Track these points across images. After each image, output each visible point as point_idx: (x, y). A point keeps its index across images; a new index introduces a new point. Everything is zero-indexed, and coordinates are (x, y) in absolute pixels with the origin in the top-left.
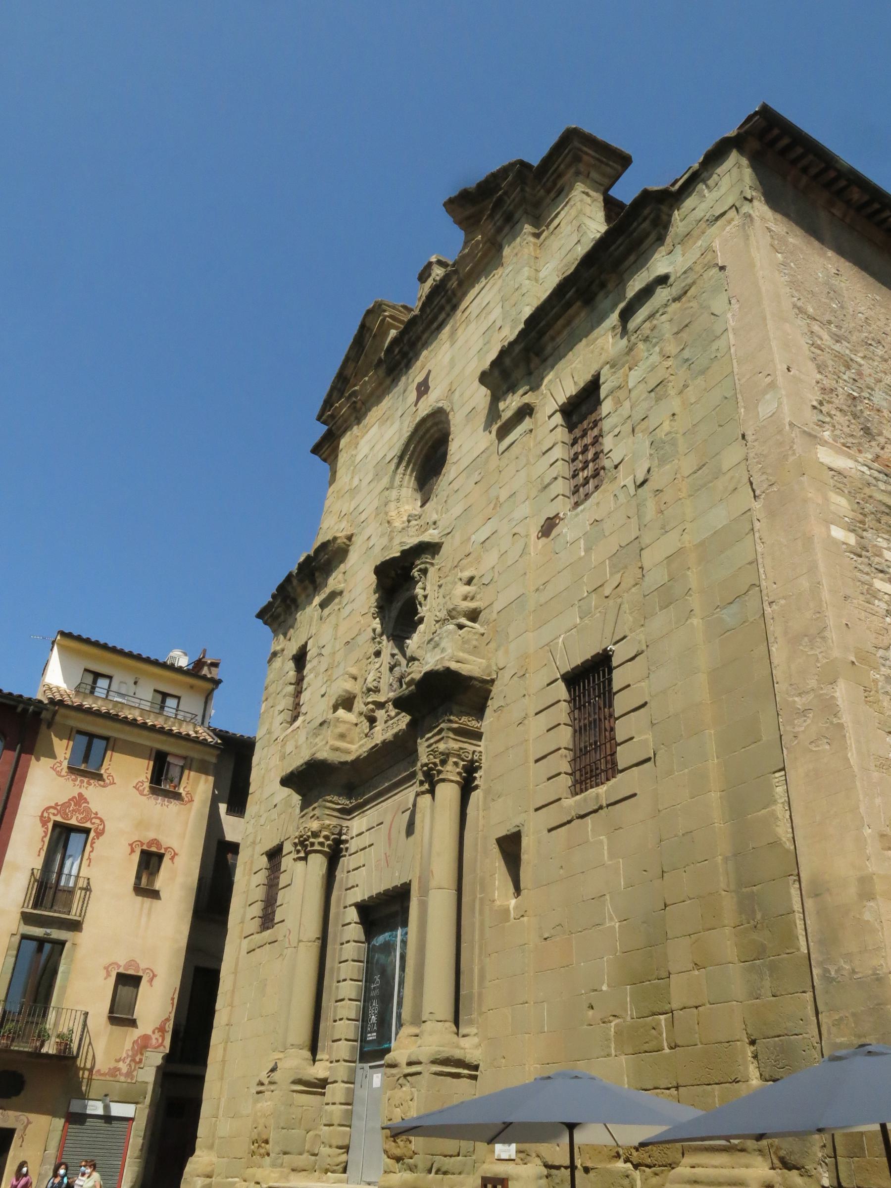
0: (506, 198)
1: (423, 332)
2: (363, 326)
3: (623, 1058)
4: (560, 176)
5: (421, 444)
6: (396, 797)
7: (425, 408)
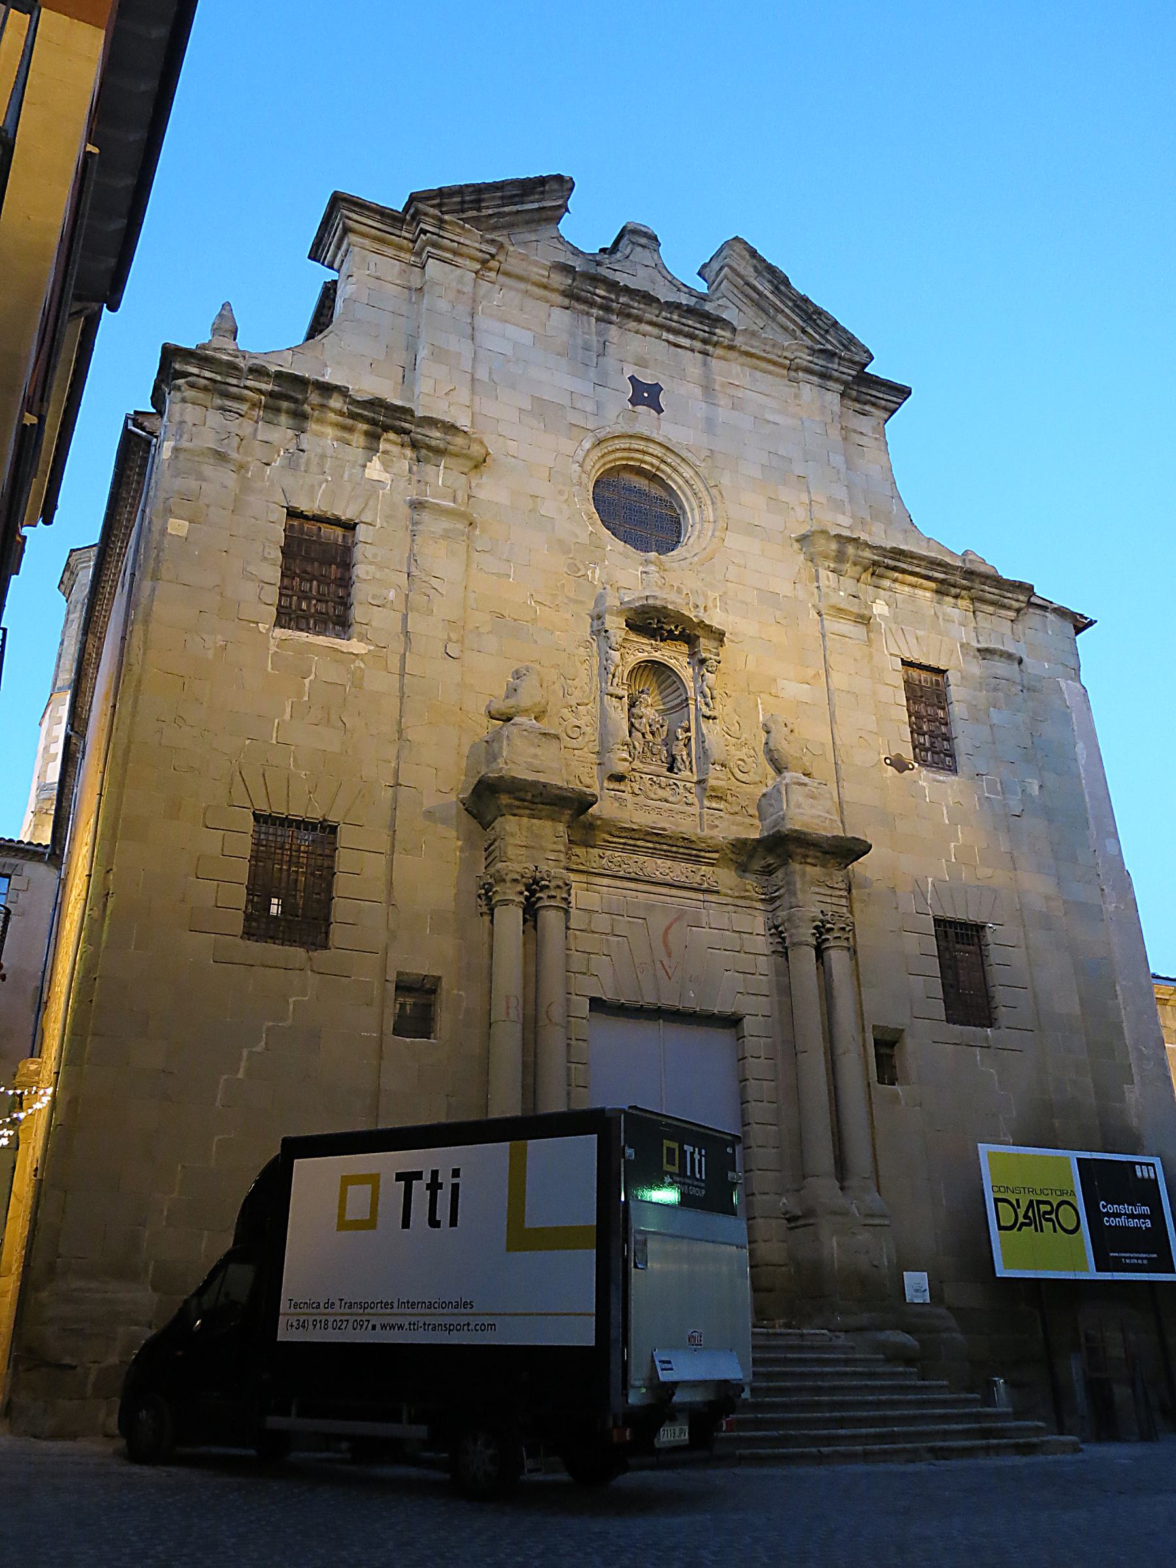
1: (651, 323)
2: (542, 181)
4: (874, 404)
5: (626, 454)
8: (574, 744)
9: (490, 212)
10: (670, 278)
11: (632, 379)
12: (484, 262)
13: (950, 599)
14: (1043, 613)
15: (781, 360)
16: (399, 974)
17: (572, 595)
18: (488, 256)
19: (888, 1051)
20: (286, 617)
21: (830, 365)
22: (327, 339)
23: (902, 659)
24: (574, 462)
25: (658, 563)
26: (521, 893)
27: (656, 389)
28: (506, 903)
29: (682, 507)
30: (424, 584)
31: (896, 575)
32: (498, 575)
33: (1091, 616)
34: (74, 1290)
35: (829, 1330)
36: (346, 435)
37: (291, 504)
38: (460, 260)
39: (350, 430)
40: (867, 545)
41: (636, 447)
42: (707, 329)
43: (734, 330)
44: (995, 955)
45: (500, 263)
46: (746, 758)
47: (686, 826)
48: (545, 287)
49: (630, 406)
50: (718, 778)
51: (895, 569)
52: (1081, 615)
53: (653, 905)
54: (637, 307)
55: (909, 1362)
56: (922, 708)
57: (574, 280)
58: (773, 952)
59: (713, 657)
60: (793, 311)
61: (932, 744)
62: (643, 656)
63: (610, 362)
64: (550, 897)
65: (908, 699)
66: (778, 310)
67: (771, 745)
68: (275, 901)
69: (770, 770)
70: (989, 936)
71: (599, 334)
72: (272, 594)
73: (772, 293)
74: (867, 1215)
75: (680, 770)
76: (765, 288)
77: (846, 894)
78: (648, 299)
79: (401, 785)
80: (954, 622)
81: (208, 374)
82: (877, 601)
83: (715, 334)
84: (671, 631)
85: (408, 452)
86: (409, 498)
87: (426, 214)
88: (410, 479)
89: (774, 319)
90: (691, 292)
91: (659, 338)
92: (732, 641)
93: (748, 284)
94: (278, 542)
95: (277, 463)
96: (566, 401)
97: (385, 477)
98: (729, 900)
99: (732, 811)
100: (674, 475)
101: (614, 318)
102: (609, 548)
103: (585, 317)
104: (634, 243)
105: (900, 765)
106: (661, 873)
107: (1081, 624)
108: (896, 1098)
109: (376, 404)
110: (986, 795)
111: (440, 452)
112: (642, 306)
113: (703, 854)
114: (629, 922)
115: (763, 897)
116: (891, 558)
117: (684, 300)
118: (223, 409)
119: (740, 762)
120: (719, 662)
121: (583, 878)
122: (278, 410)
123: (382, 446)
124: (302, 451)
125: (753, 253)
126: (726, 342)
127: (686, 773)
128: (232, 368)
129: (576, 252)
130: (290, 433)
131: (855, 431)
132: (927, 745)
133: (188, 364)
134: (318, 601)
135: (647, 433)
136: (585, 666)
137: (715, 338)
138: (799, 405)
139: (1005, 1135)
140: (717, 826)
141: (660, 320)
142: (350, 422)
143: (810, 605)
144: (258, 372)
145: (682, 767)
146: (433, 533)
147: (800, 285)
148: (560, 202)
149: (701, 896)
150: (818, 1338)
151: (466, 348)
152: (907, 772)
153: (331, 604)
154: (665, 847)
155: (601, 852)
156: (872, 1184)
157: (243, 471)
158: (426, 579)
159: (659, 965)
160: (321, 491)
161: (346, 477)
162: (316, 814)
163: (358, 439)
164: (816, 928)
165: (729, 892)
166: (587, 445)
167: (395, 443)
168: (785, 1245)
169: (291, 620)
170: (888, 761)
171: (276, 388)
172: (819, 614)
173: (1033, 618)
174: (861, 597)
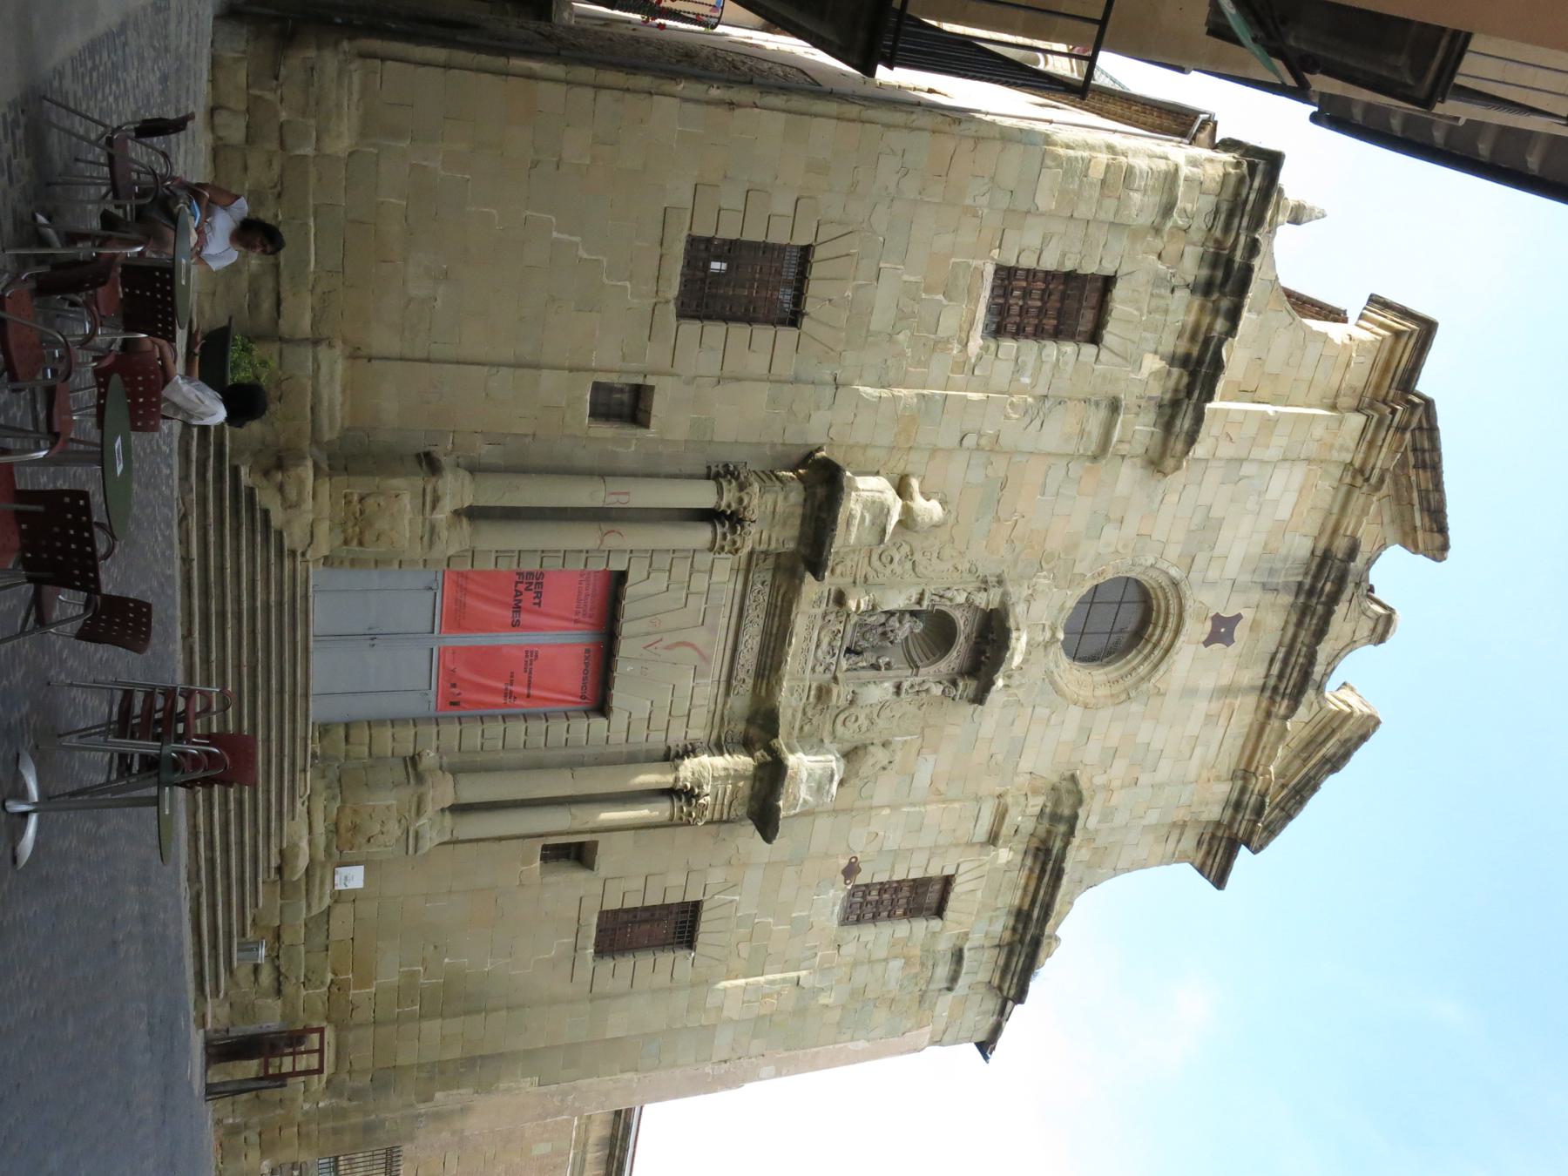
0: (1253, 818)
2: (1442, 529)
3: (397, 978)
4: (1208, 853)
5: (1163, 609)
7: (1196, 629)
8: (875, 557)
9: (1413, 478)
10: (1342, 654)
11: (1238, 617)
12: (1361, 471)
13: (1011, 923)
14: (997, 1012)
15: (1255, 764)
16: (652, 388)
18: (1367, 475)
19: (572, 855)
20: (1006, 276)
21: (1248, 811)
22: (1284, 314)
23: (953, 876)
24: (1156, 558)
26: (729, 506)
27: (1228, 639)
28: (720, 493)
29: (1109, 663)
31: (1037, 871)
32: (1045, 485)
33: (994, 1057)
34: (351, 77)
35: (309, 796)
36: (1187, 335)
37: (1119, 281)
38: (1364, 447)
39: (1193, 338)
40: (1066, 844)
41: (1171, 620)
42: (1288, 691)
43: (1286, 717)
44: (665, 959)
45: (1360, 488)
46: (857, 724)
47: (791, 664)
48: (1335, 531)
49: (1211, 615)
50: (839, 696)
51: (1043, 871)
52: (994, 1049)
53: (716, 634)
54: (1312, 623)
55: (279, 870)
56: (905, 892)
57: (1341, 561)
58: (669, 748)
59: (959, 692)
60: (1304, 777)
61: (871, 903)
62: (961, 624)
63: (1256, 595)
64: (724, 536)
65: (914, 880)
66: (1305, 761)
67: (871, 749)
68: (724, 266)
69: (847, 747)
70: (682, 954)
71: (1286, 584)
72: (1028, 262)
73: (1324, 756)
74: (417, 833)
76: (1330, 748)
77: (725, 817)
78: (1320, 633)
79: (837, 388)
80: (990, 926)
81: (1252, 197)
82: (1012, 853)
83: (1283, 698)
84: (984, 652)
85: (1168, 396)
86: (1123, 396)
87: (1412, 414)
88: (1142, 398)
89: (1296, 757)
90: (1327, 675)
91: (1280, 644)
93: (1333, 732)
94: (1081, 267)
95: (1161, 267)
96: (1216, 552)
97: (1145, 372)
98: (719, 706)
99: (807, 710)
100: (1140, 657)
101: (1302, 599)
102: (1069, 593)
103: (1302, 571)
104: (1377, 620)
105: (851, 871)
107: (985, 1047)
108: (528, 861)
109: (1218, 366)
110: (819, 954)
111: (1168, 427)
112: (1313, 627)
113: (765, 682)
114: (700, 610)
115: (723, 739)
116: (1053, 869)
117: (1318, 670)
118: (1217, 212)
119: (854, 718)
120: (953, 699)
121: (743, 566)
122: (1214, 266)
123: (1176, 371)
124: (1173, 291)
125: (1364, 738)
126: (1274, 710)
127: (844, 664)
128: (1257, 221)
129: (1370, 563)
130: (1190, 279)
131: (1182, 834)
132: (869, 898)
133: (1264, 178)
134: (1021, 307)
135: (1184, 631)
136: (951, 569)
137: (1278, 699)
138: (1209, 780)
139: (491, 964)
140: (792, 695)
141: (1298, 645)
142: (1201, 338)
144: (1253, 248)
145: (851, 661)
146: (1087, 421)
147: (1332, 785)
148: (1421, 546)
149: (723, 678)
150: (303, 784)
151: (1272, 453)
152: (842, 878)
153: (1018, 319)
154: (772, 645)
155: (768, 582)
156: (447, 838)
157: (1153, 232)
158: (1041, 413)
159: (658, 637)
160: (1131, 310)
161: (1147, 335)
162: (810, 306)
163: (1182, 347)
164: (692, 789)
165: (728, 706)
166: (1173, 572)
167: (1178, 383)
168: (390, 754)
169: (1003, 280)
170: (853, 860)
171: (1236, 266)
172: (1000, 796)
173: (992, 1004)
174: (1016, 837)
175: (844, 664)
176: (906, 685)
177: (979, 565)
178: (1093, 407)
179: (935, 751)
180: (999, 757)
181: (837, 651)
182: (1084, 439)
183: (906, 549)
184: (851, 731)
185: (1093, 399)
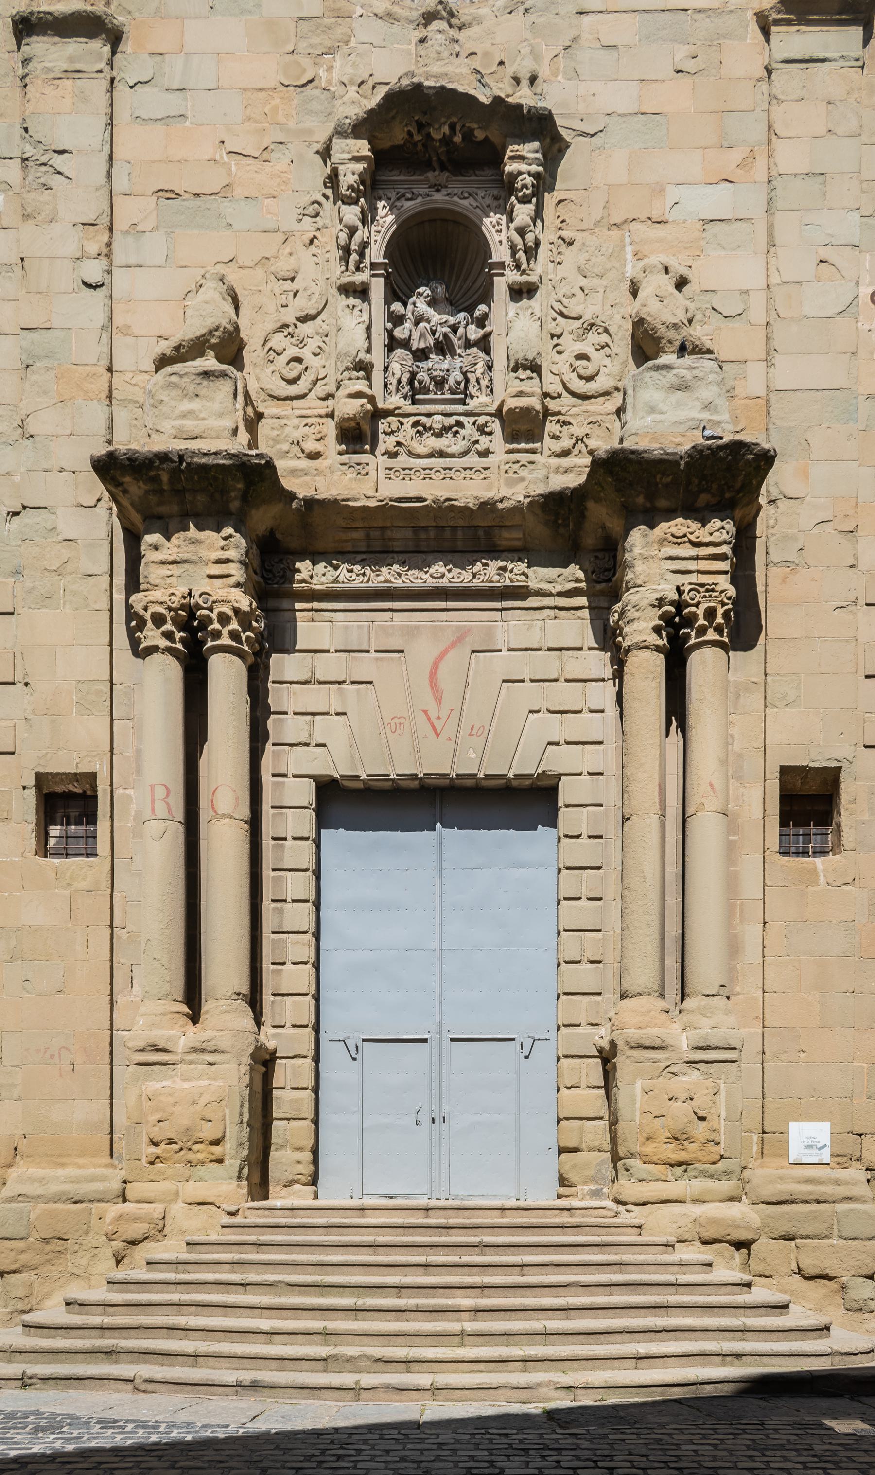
6: (443, 615)
8: (293, 390)
17: (291, 124)
25: (445, 14)
30: (43, 168)
53: (418, 627)
75: (472, 397)
79: (24, 507)
92: (584, 134)
102: (359, 11)
106: (431, 576)
114: (377, 659)
143: (750, 14)
146: (49, 70)
158: (44, 159)
175: (473, 404)
176: (512, 276)
177: (307, 199)
178: (31, 66)
179: (660, 190)
180: (681, 53)
181: (451, 420)
182: (78, 66)
183: (278, 341)
184: (607, 361)
185: (21, 72)
